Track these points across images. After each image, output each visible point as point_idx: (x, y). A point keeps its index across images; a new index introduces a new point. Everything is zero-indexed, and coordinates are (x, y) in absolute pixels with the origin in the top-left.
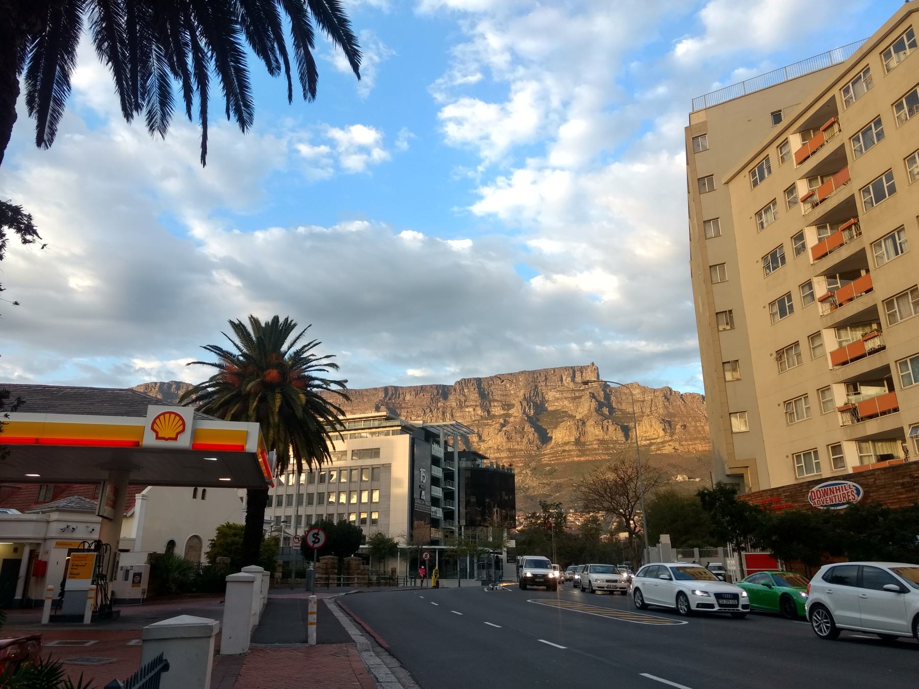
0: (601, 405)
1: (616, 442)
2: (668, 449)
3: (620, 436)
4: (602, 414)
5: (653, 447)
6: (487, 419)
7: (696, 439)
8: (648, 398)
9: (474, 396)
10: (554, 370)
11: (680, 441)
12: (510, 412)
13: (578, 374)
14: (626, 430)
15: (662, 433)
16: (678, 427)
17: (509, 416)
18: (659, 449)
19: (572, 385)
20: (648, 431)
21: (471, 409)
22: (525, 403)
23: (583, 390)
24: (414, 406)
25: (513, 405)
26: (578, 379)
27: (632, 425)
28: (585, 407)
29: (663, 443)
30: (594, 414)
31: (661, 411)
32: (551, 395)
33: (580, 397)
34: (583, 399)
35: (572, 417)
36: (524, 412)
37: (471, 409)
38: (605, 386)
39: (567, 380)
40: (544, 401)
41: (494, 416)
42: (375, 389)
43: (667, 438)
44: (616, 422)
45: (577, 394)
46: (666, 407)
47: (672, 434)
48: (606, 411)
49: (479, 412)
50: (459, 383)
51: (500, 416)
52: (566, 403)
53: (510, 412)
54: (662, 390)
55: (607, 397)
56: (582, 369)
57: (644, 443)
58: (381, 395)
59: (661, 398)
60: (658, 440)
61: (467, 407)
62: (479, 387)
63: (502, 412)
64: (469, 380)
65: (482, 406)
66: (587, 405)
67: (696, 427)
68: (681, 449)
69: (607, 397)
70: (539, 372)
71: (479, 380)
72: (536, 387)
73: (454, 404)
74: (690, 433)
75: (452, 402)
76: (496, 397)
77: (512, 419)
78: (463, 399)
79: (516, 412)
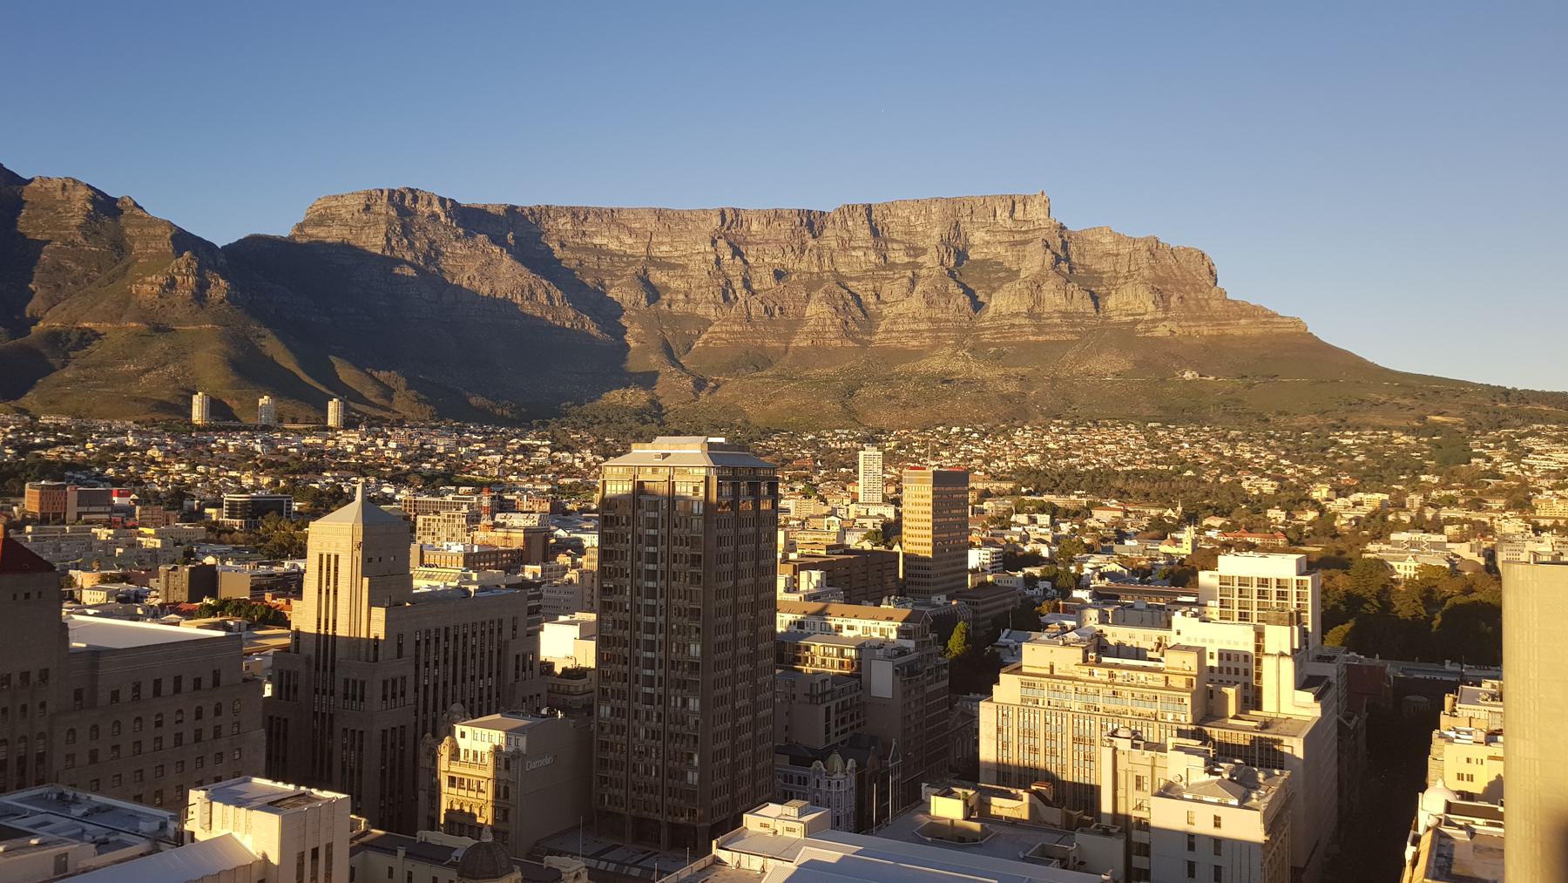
0: (1058, 260)
2: (1161, 331)
3: (1089, 304)
5: (1139, 327)
6: (884, 269)
7: (1200, 318)
8: (1125, 250)
9: (864, 233)
11: (1177, 319)
12: (920, 260)
13: (1019, 207)
15: (1151, 307)
16: (1174, 299)
17: (920, 266)
18: (1148, 330)
19: (1009, 224)
20: (1129, 302)
21: (860, 253)
23: (1026, 232)
24: (767, 242)
25: (924, 251)
26: (1019, 214)
27: (1103, 289)
28: (1035, 261)
29: (1154, 321)
30: (1051, 272)
31: (1146, 273)
32: (978, 237)
33: (1025, 243)
34: (1030, 248)
35: (1013, 275)
36: (942, 264)
37: (860, 253)
38: (1062, 228)
39: (1003, 215)
40: (967, 245)
41: (893, 266)
42: (705, 211)
43: (1160, 315)
44: (1082, 282)
45: (1017, 237)
46: (1153, 268)
47: (1166, 309)
48: (1064, 266)
49: (873, 258)
50: (841, 211)
52: (1001, 249)
53: (920, 260)
55: (1065, 246)
57: (1124, 319)
58: (717, 221)
60: (1147, 317)
61: (854, 249)
62: (869, 215)
63: (907, 260)
66: (1039, 258)
67: (1198, 301)
68: (1179, 332)
69: (1065, 246)
70: (962, 201)
71: (869, 209)
73: (834, 244)
74: (1189, 309)
75: (830, 237)
77: (924, 272)
78: (846, 236)
79: (929, 260)
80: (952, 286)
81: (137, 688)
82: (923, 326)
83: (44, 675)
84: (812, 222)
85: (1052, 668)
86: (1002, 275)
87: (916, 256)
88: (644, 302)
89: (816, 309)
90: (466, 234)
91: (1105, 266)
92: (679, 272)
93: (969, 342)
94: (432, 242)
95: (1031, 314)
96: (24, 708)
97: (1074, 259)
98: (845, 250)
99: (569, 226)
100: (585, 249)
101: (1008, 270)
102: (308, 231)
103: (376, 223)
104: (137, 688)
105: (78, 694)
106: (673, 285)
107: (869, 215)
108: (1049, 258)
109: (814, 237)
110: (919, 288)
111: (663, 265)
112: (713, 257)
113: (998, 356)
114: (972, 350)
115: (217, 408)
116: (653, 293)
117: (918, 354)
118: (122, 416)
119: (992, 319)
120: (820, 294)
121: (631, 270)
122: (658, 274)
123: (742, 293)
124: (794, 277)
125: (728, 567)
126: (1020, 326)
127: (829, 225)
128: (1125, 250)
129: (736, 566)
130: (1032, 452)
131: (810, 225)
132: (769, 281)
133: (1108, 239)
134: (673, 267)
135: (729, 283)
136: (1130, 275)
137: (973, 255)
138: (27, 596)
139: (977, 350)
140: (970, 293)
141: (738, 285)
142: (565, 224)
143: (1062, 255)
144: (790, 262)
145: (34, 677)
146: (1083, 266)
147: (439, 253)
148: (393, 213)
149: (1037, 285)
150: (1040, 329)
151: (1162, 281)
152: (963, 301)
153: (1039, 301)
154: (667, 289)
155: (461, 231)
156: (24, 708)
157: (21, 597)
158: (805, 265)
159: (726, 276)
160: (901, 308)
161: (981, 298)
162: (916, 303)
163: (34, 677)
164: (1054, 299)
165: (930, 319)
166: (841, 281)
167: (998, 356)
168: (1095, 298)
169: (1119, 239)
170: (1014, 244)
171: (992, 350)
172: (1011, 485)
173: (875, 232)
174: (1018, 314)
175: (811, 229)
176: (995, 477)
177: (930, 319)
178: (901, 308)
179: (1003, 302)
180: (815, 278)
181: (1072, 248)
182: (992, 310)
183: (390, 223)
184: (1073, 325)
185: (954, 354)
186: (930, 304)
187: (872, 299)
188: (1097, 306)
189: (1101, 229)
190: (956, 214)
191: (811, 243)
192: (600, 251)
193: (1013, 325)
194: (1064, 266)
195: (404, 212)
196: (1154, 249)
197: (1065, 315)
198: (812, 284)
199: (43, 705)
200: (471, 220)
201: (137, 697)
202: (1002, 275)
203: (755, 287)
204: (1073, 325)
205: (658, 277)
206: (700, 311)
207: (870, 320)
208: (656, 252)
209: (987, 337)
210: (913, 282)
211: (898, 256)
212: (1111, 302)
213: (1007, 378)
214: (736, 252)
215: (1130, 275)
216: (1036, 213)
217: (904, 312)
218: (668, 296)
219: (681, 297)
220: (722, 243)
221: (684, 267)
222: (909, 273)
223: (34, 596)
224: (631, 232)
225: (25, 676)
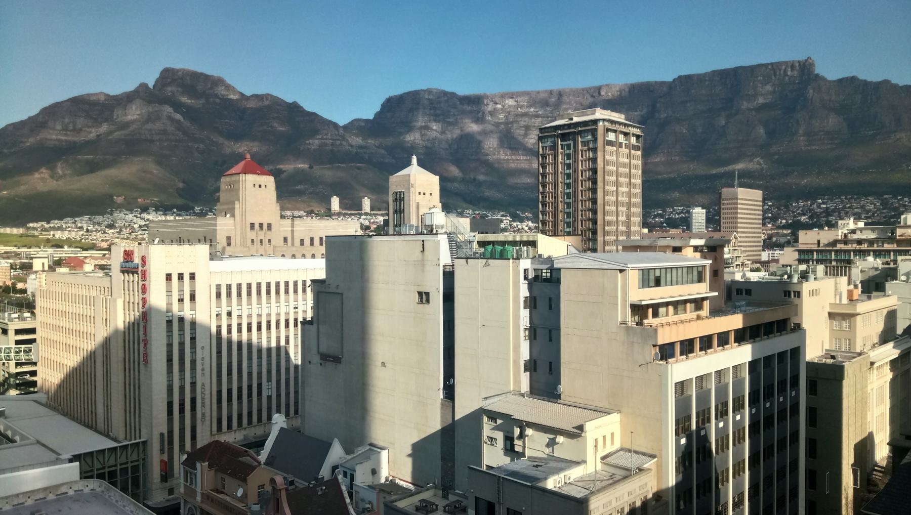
81: (312, 239)
83: (269, 226)
85: (819, 241)
96: (261, 241)
100: (525, 115)
104: (312, 239)
105: (285, 239)
115: (342, 205)
118: (299, 210)
125: (613, 178)
129: (617, 179)
130: (804, 215)
138: (260, 186)
145: (265, 227)
156: (261, 241)
157: (257, 186)
163: (265, 227)
172: (789, 231)
176: (779, 227)
199: (270, 241)
201: (312, 243)
223: (263, 186)
225: (261, 225)
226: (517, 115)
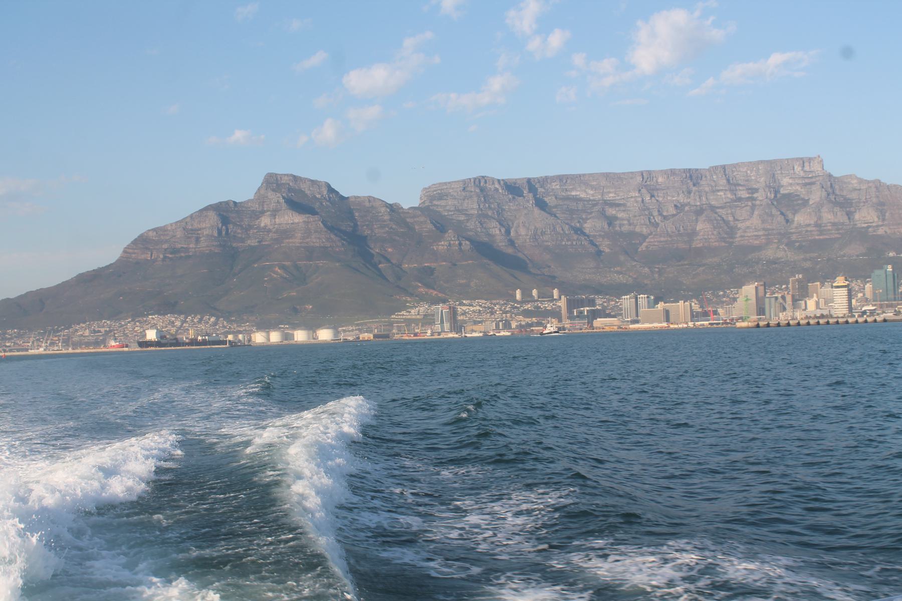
1: (843, 224)
3: (844, 219)
4: (830, 201)
6: (735, 201)
8: (864, 187)
10: (788, 160)
12: (755, 195)
13: (806, 164)
14: (849, 215)
19: (802, 174)
20: (866, 216)
22: (767, 190)
23: (811, 178)
25: (756, 190)
26: (807, 168)
28: (816, 196)
31: (874, 200)
32: (785, 181)
34: (814, 188)
38: (830, 176)
39: (798, 169)
41: (740, 199)
45: (807, 181)
46: (877, 197)
49: (729, 195)
50: (709, 170)
51: (748, 199)
52: (798, 188)
53: (755, 195)
54: (874, 182)
56: (810, 160)
58: (639, 179)
59: (874, 189)
61: (718, 191)
62: (725, 171)
64: (716, 167)
65: (731, 190)
71: (724, 167)
72: (774, 175)
73: (707, 189)
76: (740, 182)
77: (758, 202)
78: (713, 184)
80: (774, 211)
82: (761, 233)
84: (692, 177)
86: (800, 202)
87: (753, 193)
88: (606, 226)
89: (702, 226)
90: (514, 198)
91: (854, 195)
92: (622, 208)
93: (785, 240)
94: (498, 205)
95: (817, 225)
97: (837, 192)
98: (713, 192)
99: (558, 187)
100: (568, 198)
101: (803, 199)
102: (435, 202)
103: (471, 197)
106: (620, 215)
107: (725, 171)
108: (824, 194)
109: (694, 185)
110: (756, 213)
111: (613, 204)
112: (640, 199)
113: (800, 247)
114: (786, 245)
116: (611, 221)
117: (759, 248)
119: (796, 228)
120: (703, 217)
121: (596, 208)
122: (610, 210)
123: (658, 219)
124: (687, 208)
126: (811, 231)
127: (704, 179)
128: (864, 187)
131: (691, 177)
132: (672, 211)
133: (855, 181)
134: (618, 205)
135: (651, 214)
136: (866, 202)
137: (782, 191)
139: (790, 244)
140: (782, 214)
141: (655, 213)
142: (556, 186)
143: (830, 190)
144: (682, 199)
146: (842, 196)
147: (503, 210)
148: (478, 190)
149: (819, 207)
150: (821, 232)
151: (882, 204)
152: (781, 219)
153: (820, 218)
154: (616, 218)
155: (510, 196)
158: (695, 201)
159: (649, 209)
160: (748, 223)
161: (790, 216)
162: (755, 221)
164: (827, 217)
165: (764, 229)
166: (713, 208)
167: (800, 247)
168: (849, 215)
169: (861, 181)
170: (805, 185)
171: (797, 244)
173: (728, 180)
174: (809, 225)
175: (691, 180)
177: (764, 229)
178: (748, 223)
179: (801, 219)
180: (698, 208)
181: (837, 187)
182: (796, 222)
183: (478, 196)
184: (838, 229)
185: (778, 248)
186: (763, 222)
187: (731, 218)
188: (849, 218)
189: (851, 175)
190: (772, 167)
191: (694, 189)
192: (577, 199)
193: (807, 231)
194: (832, 197)
195: (482, 190)
196: (878, 185)
197: (834, 224)
198: (699, 212)
200: (512, 188)
202: (800, 202)
203: (665, 214)
204: (838, 229)
205: (611, 211)
206: (638, 229)
207: (732, 231)
208: (607, 197)
209: (794, 237)
210: (753, 207)
211: (744, 194)
212: (857, 216)
213: (805, 260)
214: (652, 196)
215: (866, 202)
216: (816, 167)
217: (750, 225)
218: (618, 222)
219: (625, 222)
220: (644, 191)
221: (624, 205)
222: (750, 204)
224: (592, 188)
226: (561, 199)
